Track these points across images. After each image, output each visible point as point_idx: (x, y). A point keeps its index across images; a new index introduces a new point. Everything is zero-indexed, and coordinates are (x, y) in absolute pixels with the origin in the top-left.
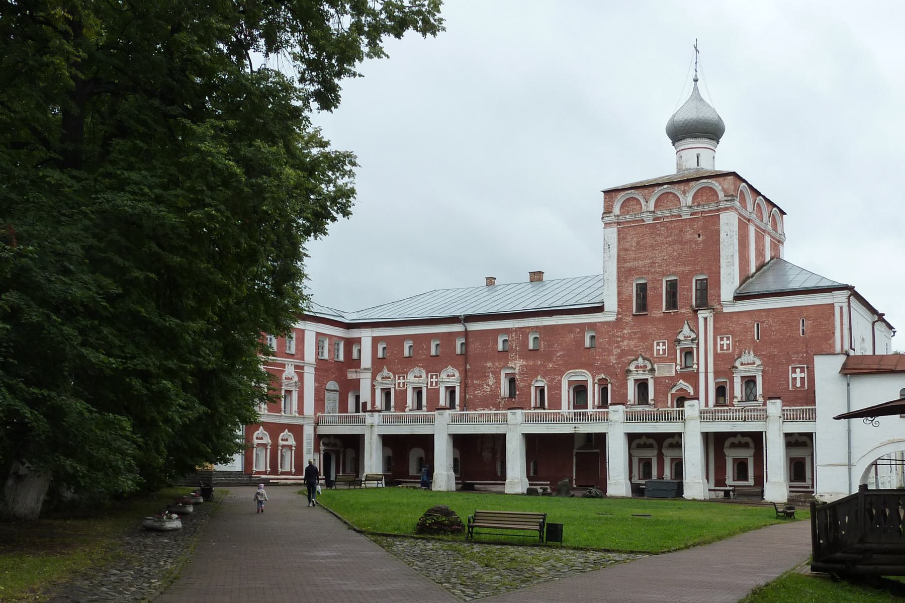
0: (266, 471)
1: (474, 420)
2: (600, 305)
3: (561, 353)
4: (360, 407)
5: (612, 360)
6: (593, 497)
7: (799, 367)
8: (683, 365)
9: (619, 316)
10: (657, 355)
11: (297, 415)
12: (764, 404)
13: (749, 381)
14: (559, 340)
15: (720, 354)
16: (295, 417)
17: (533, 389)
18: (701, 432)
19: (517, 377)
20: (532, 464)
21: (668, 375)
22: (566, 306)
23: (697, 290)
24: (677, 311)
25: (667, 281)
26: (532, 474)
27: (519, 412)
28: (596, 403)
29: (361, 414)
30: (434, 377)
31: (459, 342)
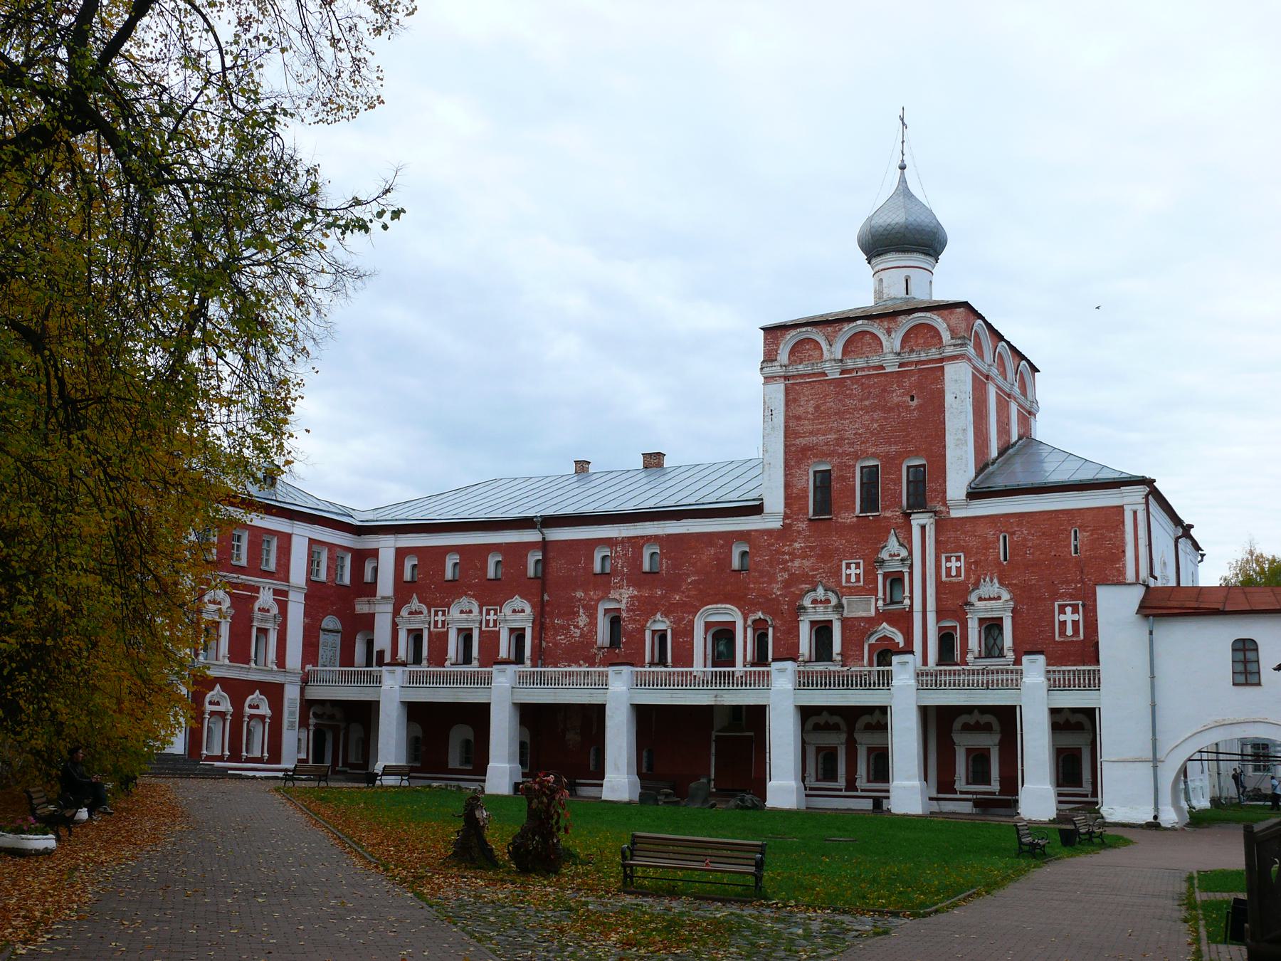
0: (223, 755)
1: (555, 681)
2: (758, 503)
4: (375, 658)
5: (774, 591)
6: (748, 808)
7: (1070, 605)
8: (888, 600)
9: (787, 521)
10: (846, 582)
11: (275, 668)
12: (1018, 662)
13: (992, 627)
15: (945, 583)
16: (272, 670)
17: (648, 635)
18: (919, 706)
19: (624, 614)
20: (645, 754)
21: (864, 615)
22: (703, 504)
23: (908, 482)
24: (877, 514)
25: (862, 468)
26: (644, 770)
27: (626, 670)
28: (749, 658)
29: (375, 668)
30: (492, 612)
31: (534, 557)
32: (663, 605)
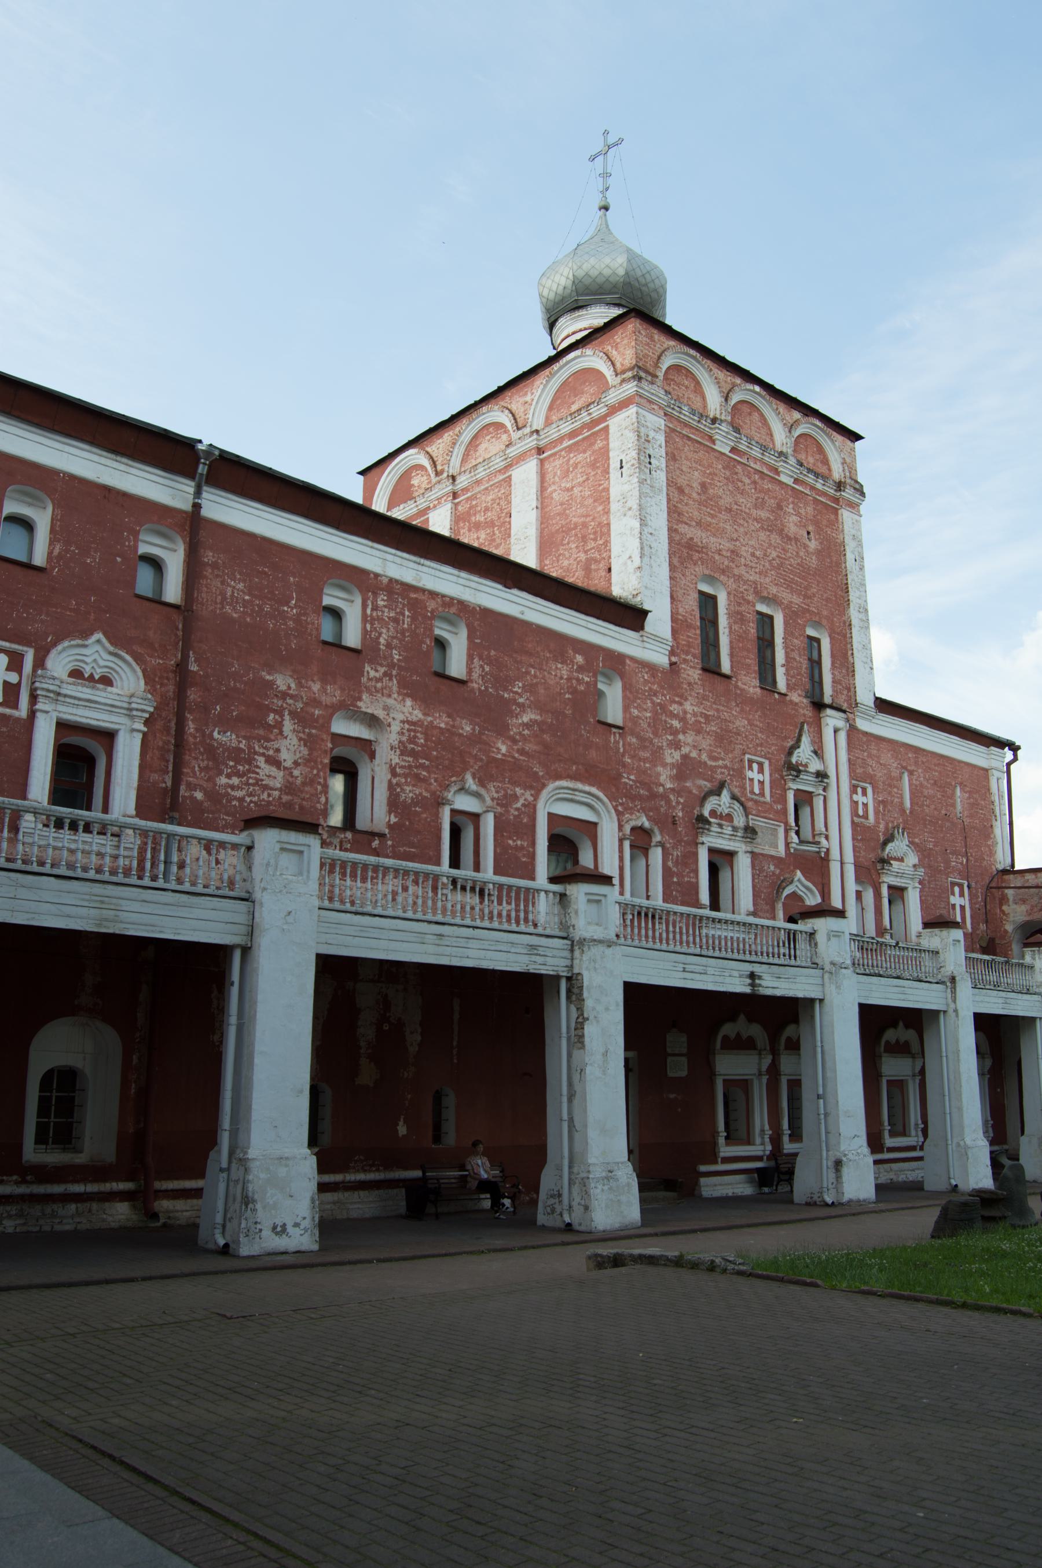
3: (533, 717)
9: (674, 659)
14: (528, 673)
32: (476, 758)
